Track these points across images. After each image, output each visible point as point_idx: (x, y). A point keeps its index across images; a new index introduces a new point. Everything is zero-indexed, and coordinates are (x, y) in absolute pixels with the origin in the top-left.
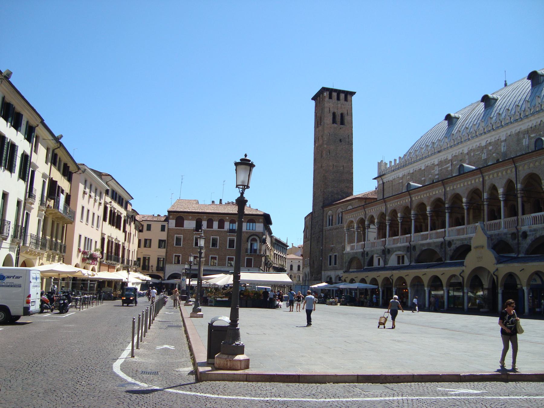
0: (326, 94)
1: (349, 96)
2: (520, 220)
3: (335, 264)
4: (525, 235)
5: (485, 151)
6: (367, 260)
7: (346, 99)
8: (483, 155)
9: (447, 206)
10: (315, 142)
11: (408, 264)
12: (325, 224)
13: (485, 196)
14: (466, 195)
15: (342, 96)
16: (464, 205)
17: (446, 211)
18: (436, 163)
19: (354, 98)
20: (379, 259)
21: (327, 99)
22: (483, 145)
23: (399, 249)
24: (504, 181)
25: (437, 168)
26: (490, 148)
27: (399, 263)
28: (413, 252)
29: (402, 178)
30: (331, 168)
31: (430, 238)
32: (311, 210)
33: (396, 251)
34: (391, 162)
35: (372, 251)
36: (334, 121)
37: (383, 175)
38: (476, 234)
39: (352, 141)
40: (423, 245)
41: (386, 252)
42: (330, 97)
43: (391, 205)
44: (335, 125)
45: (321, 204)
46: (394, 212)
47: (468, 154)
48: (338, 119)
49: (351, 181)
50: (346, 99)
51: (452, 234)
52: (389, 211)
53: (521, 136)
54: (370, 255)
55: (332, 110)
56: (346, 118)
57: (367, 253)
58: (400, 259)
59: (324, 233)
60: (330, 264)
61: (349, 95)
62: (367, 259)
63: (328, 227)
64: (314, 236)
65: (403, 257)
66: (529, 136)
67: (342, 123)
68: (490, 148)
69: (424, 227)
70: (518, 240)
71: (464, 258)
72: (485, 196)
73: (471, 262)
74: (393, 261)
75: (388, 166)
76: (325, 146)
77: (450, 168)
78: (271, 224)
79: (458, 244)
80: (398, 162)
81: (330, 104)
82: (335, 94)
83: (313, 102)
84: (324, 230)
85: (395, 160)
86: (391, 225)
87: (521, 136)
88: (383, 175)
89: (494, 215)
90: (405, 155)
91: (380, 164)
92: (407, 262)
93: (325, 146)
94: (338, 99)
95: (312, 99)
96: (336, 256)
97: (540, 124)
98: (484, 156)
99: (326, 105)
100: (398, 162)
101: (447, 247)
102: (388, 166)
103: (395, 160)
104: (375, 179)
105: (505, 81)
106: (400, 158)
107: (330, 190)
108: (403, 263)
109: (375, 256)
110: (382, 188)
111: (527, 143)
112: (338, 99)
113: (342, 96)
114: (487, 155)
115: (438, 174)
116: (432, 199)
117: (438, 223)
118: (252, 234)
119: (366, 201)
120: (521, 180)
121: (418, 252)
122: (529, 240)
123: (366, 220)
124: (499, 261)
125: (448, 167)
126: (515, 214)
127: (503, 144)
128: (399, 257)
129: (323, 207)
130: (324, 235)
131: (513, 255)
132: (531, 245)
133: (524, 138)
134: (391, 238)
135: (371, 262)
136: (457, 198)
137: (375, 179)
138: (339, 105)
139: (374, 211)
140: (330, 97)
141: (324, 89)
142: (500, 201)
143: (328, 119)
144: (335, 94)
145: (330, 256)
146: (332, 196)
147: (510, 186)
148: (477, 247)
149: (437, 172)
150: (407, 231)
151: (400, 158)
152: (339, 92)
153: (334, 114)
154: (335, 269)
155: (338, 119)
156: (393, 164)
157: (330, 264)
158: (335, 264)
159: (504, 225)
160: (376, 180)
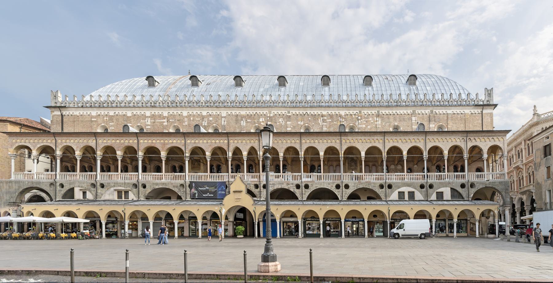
8: (204, 122)
23: (116, 184)
24: (248, 147)
33: (114, 186)
40: (157, 184)
65: (126, 193)
69: (112, 167)
74: (110, 194)
87: (240, 118)
92: (131, 196)
105: (535, 106)
111: (244, 124)
121: (148, 190)
127: (223, 119)
128: (119, 193)
136: (237, 151)
147: (252, 151)
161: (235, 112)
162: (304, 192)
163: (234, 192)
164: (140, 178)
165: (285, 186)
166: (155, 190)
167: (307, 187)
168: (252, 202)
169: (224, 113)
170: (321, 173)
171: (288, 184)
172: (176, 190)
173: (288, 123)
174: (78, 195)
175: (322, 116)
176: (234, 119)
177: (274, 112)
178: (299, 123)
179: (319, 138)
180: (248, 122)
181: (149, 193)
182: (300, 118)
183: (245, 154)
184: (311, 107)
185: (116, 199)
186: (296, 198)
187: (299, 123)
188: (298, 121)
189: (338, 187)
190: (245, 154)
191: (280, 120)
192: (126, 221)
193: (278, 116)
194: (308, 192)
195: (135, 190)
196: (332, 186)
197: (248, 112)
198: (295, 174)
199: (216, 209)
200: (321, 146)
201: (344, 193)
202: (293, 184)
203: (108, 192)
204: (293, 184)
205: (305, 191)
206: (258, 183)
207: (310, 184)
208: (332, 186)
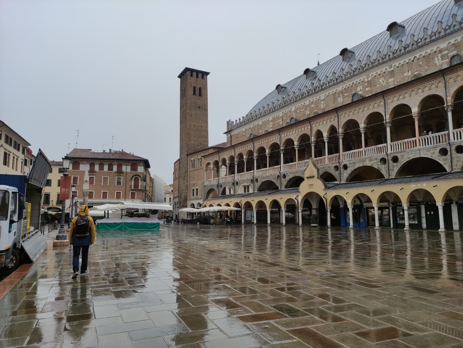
0: (188, 73)
1: (205, 75)
2: (341, 156)
3: (197, 195)
4: (345, 167)
5: (308, 108)
6: (221, 191)
7: (203, 77)
8: (307, 112)
9: (281, 148)
10: (181, 108)
11: (252, 192)
12: (189, 166)
13: (313, 139)
14: (297, 139)
15: (200, 75)
16: (295, 146)
17: (281, 152)
18: (271, 119)
19: (208, 77)
20: (230, 190)
21: (189, 77)
22: (306, 104)
25: (271, 123)
26: (312, 106)
27: (245, 192)
28: (256, 183)
29: (245, 132)
30: (193, 127)
31: (269, 173)
32: (179, 158)
33: (242, 183)
34: (236, 121)
35: (225, 183)
36: (194, 94)
37: (231, 130)
38: (308, 168)
40: (264, 178)
41: (235, 184)
42: (192, 76)
43: (239, 150)
44: (195, 97)
45: (186, 153)
46: (241, 155)
47: (295, 111)
48: (197, 92)
49: (206, 137)
50: (203, 77)
51: (287, 170)
52: (237, 154)
53: (337, 95)
54: (223, 187)
55: (193, 85)
56: (203, 91)
57: (221, 186)
58: (246, 188)
60: (193, 195)
61: (205, 74)
62: (221, 190)
63: (191, 169)
65: (248, 187)
66: (343, 95)
67: (200, 95)
68: (312, 106)
70: (340, 171)
71: (298, 186)
72: (313, 139)
73: (304, 189)
74: (240, 190)
75: (235, 123)
77: (281, 123)
78: (149, 167)
79: (291, 176)
80: (241, 120)
81: (192, 81)
82: (195, 74)
83: (179, 79)
84: (188, 171)
85: (240, 119)
86: (240, 165)
88: (231, 130)
89: (319, 153)
90: (247, 115)
91: (228, 123)
92: (251, 191)
94: (197, 77)
95: (179, 77)
96: (197, 189)
97: (352, 86)
98: (308, 112)
99: (189, 81)
100: (241, 120)
101: (282, 178)
102: (235, 123)
103: (240, 119)
104: (225, 133)
106: (243, 117)
107: (192, 143)
108: (248, 191)
109: (227, 188)
110: (230, 140)
111: (341, 100)
112: (197, 77)
113: (200, 75)
114: (310, 112)
115: (272, 128)
116: (270, 144)
117: (275, 162)
118: (135, 174)
119: (219, 149)
120: (342, 126)
121: (259, 183)
122: (349, 171)
123: (220, 162)
124: (327, 188)
125: (279, 122)
126: (337, 151)
127: (322, 102)
128: (245, 188)
131: (336, 182)
132: (351, 174)
133: (339, 96)
134: (239, 174)
135: (224, 192)
137: (225, 133)
138: (198, 82)
139: (226, 155)
140: (192, 76)
141: (187, 70)
142: (324, 142)
143: (190, 92)
144: (195, 74)
145: (193, 190)
148: (308, 178)
149: (271, 126)
150: (250, 168)
151: (243, 117)
152: (198, 72)
153: (194, 88)
154: (197, 199)
155: (197, 92)
156: (238, 122)
157: (193, 195)
158: (197, 195)
159: (327, 162)
160: (225, 134)
161: (332, 91)
162: (391, 168)
163: (313, 177)
164: (255, 174)
165: (368, 164)
166: (263, 183)
167: (395, 159)
168: (323, 187)
169: (322, 96)
170: (415, 136)
171: (371, 160)
172: (274, 181)
173: (390, 80)
174: (227, 193)
175: (440, 51)
176: (332, 98)
177: (373, 73)
178: (406, 74)
179: (409, 91)
180: (346, 96)
181: (260, 186)
182: (406, 68)
183: (325, 135)
184: (419, 47)
185: (243, 193)
186: (382, 176)
187: (406, 74)
188: (404, 72)
189: (444, 152)
190: (325, 135)
191: (381, 81)
192: (299, 208)
193: (378, 77)
194: (396, 168)
195: (252, 185)
196: (434, 153)
197: (344, 86)
198: (379, 146)
199: (293, 197)
200: (413, 101)
201: (454, 161)
202: (376, 159)
203: (240, 188)
204: (376, 159)
205: (393, 166)
206: (338, 164)
207: (399, 155)
208: (434, 153)
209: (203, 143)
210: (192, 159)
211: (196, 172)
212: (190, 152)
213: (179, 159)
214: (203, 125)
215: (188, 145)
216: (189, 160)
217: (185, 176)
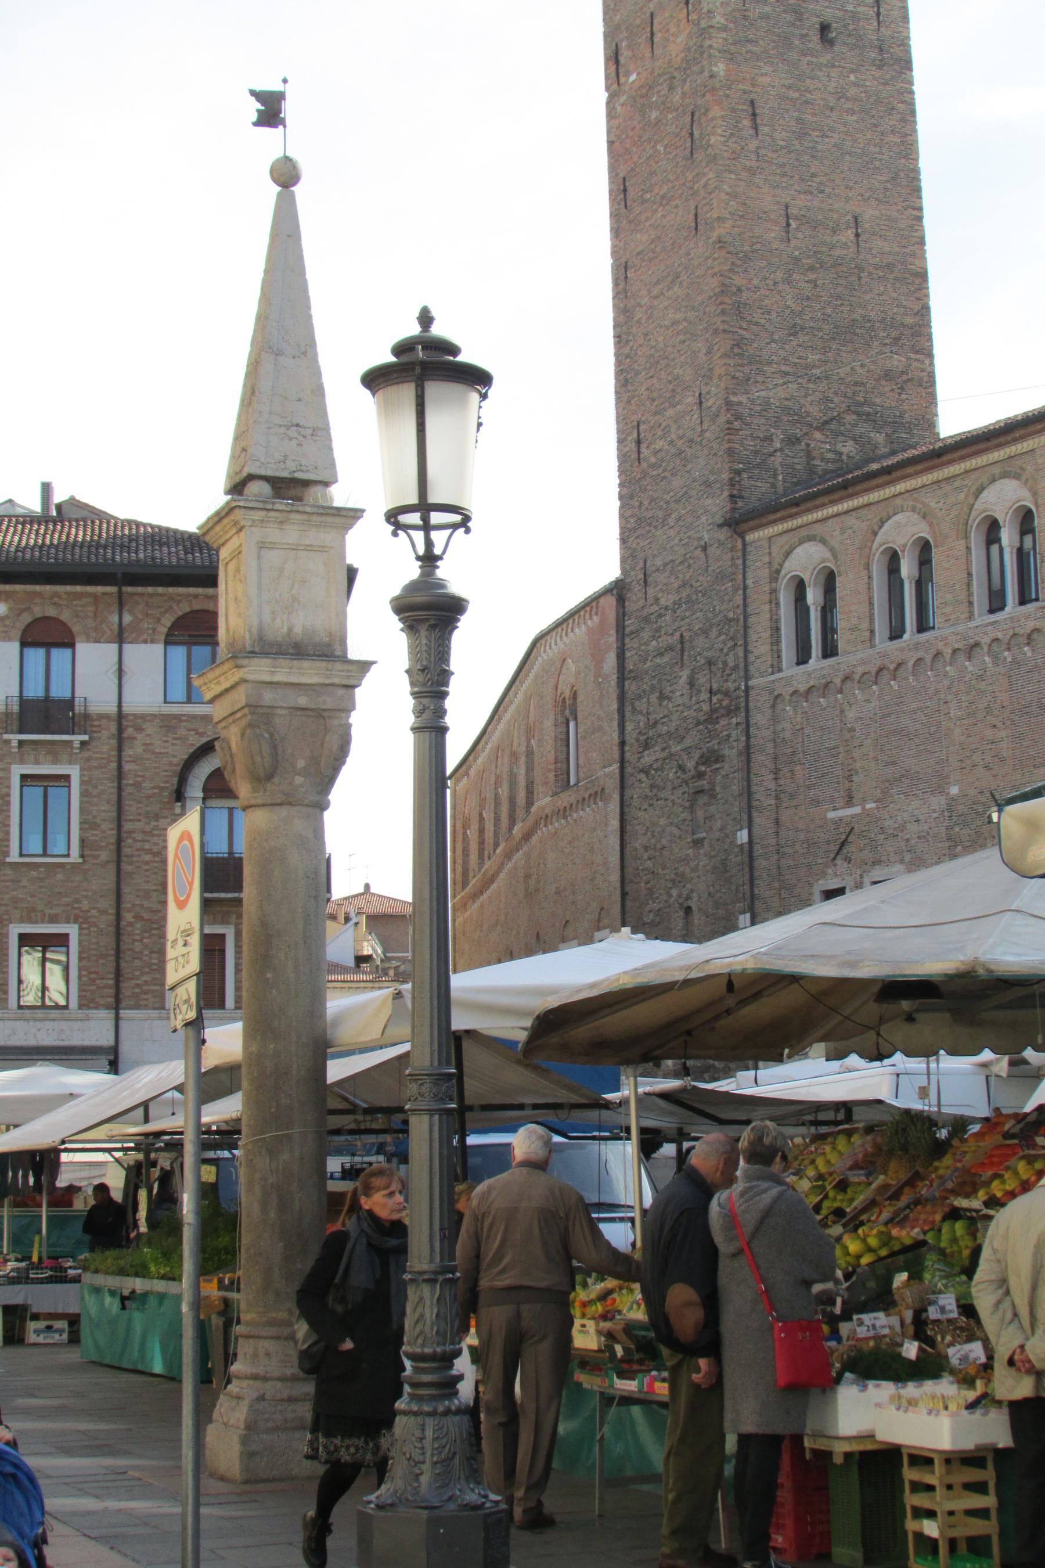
10: (614, 59)
12: (761, 648)
30: (774, 234)
32: (604, 566)
39: (904, 44)
45: (717, 505)
49: (914, 334)
59: (760, 719)
64: (647, 759)
76: (720, 68)
84: (760, 701)
93: (720, 68)
129: (739, 522)
130: (762, 734)
146: (792, 441)
209: (885, 398)
210: (806, 560)
211: (862, 706)
212: (758, 489)
213: (618, 590)
214: (869, 213)
215: (735, 420)
216: (758, 572)
217: (711, 758)
